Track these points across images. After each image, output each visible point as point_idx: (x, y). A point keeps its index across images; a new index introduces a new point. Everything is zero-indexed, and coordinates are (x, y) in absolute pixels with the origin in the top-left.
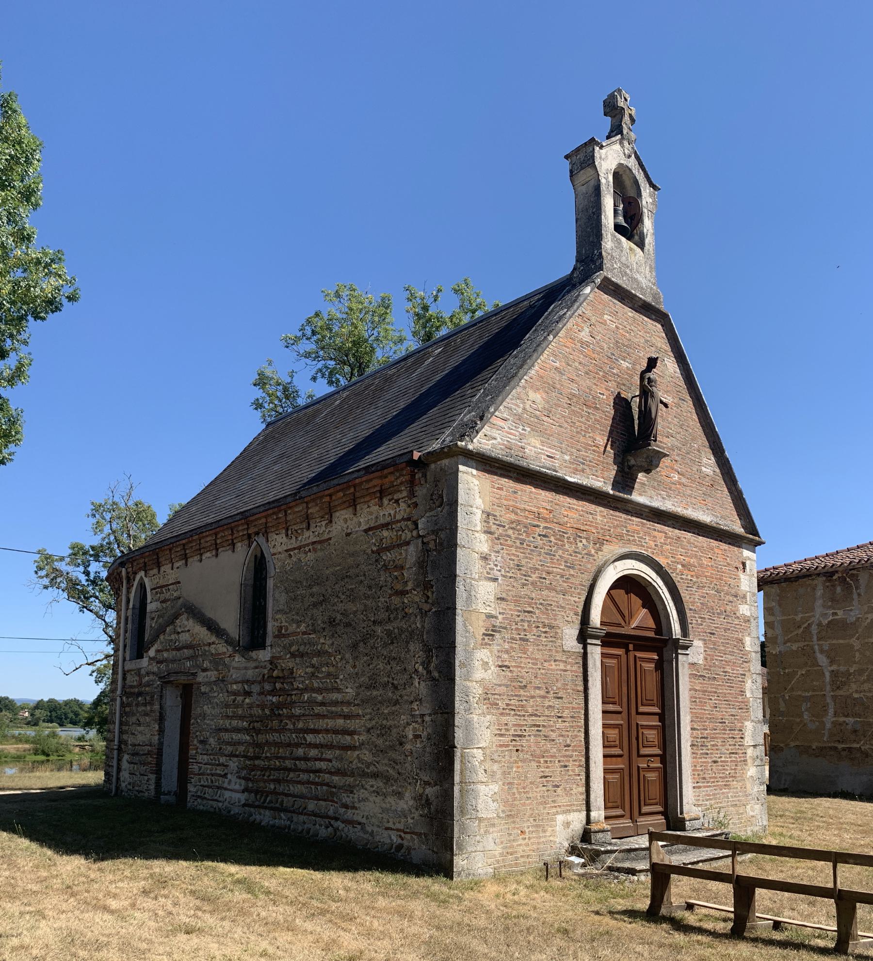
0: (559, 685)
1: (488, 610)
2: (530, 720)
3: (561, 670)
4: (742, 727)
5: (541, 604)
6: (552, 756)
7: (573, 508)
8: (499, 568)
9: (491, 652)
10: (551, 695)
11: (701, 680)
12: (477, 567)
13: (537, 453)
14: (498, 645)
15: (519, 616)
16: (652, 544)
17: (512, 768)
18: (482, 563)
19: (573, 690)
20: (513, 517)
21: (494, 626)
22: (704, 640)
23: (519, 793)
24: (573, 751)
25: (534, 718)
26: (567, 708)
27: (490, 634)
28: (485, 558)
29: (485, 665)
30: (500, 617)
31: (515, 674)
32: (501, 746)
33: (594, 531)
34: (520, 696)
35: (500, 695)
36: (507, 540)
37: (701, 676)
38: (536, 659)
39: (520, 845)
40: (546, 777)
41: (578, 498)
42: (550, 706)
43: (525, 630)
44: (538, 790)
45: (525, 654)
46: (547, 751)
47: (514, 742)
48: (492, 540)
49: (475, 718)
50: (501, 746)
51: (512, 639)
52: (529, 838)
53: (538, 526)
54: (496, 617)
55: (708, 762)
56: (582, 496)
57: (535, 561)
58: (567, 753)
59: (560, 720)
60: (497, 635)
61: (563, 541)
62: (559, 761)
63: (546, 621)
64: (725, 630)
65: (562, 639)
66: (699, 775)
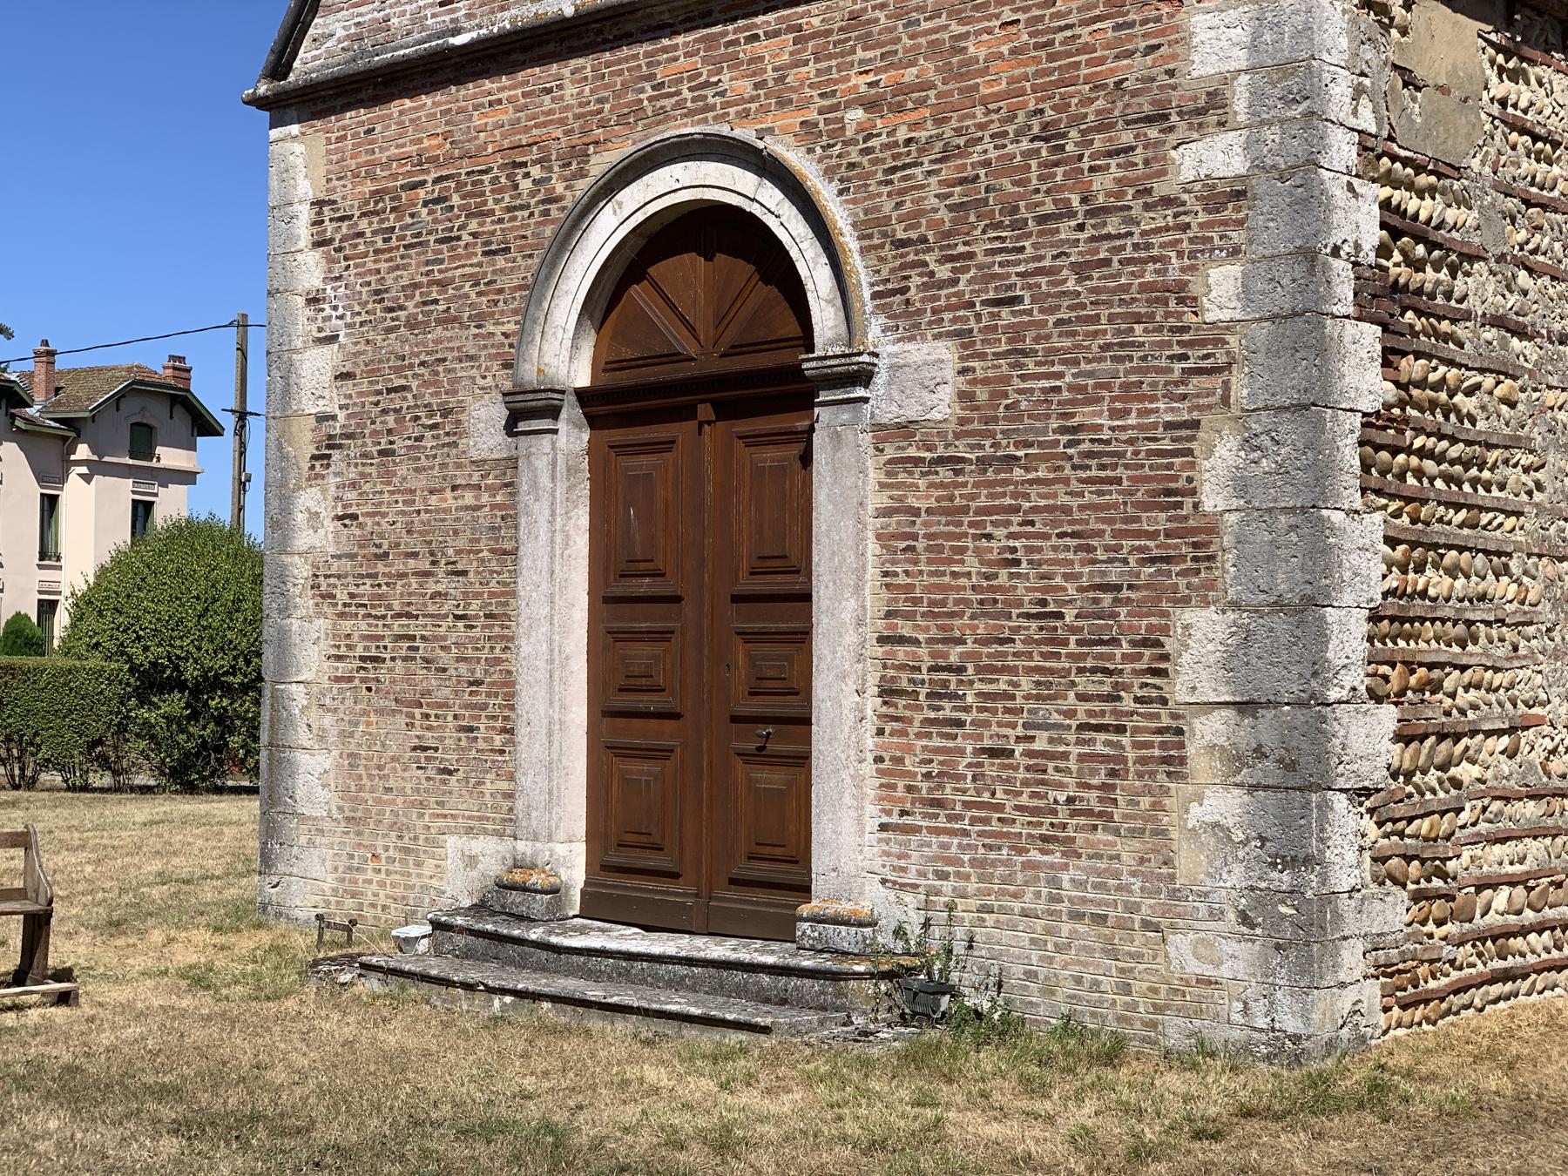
1: (322, 407)
2: (397, 626)
3: (467, 508)
4: (1165, 630)
5: (422, 364)
6: (440, 706)
7: (499, 102)
8: (341, 311)
9: (324, 491)
10: (441, 570)
11: (944, 474)
14: (336, 474)
15: (377, 404)
16: (746, 86)
17: (357, 724)
18: (309, 312)
19: (492, 551)
20: (368, 187)
21: (330, 437)
22: (958, 334)
23: (370, 776)
24: (488, 695)
25: (404, 621)
26: (478, 595)
28: (314, 301)
31: (369, 529)
32: (338, 679)
33: (559, 133)
34: (375, 576)
35: (339, 577)
36: (355, 246)
37: (941, 461)
38: (413, 492)
39: (370, 882)
40: (425, 749)
41: (511, 68)
42: (439, 594)
43: (390, 432)
44: (406, 774)
45: (389, 483)
46: (429, 692)
47: (362, 667)
48: (331, 261)
49: (295, 624)
50: (338, 679)
51: (365, 455)
52: (388, 873)
53: (423, 183)
54: (334, 418)
55: (961, 752)
56: (522, 57)
58: (474, 699)
59: (460, 624)
60: (336, 455)
61: (483, 194)
62: (455, 717)
63: (434, 401)
64: (1081, 271)
66: (909, 789)
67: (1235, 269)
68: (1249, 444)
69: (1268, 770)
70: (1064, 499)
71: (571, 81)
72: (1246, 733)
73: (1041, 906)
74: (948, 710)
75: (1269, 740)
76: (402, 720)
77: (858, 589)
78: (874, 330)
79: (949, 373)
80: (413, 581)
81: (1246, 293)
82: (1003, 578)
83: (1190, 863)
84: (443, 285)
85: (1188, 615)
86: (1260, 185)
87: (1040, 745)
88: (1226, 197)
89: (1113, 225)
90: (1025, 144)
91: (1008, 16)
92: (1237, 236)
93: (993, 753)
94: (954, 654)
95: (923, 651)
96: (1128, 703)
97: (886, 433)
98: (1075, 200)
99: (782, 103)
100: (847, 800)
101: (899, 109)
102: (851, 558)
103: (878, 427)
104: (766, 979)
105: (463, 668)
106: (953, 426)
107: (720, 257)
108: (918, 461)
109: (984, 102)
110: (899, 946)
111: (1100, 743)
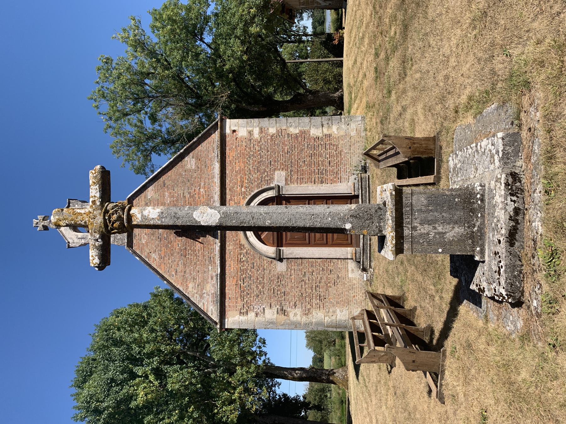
0: (300, 274)
1: (275, 313)
9: (291, 312)
12: (260, 318)
13: (212, 287)
20: (239, 299)
27: (283, 312)
28: (257, 315)
29: (295, 315)
30: (278, 307)
41: (225, 261)
48: (250, 310)
49: (314, 320)
57: (254, 287)
60: (284, 308)
64: (268, 151)
65: (282, 272)
67: (270, 129)
68: (291, 126)
69: (330, 122)
71: (229, 247)
72: (325, 126)
74: (324, 172)
75: (326, 122)
76: (330, 289)
78: (272, 185)
80: (306, 286)
81: (273, 127)
82: (306, 163)
83: (342, 133)
84: (257, 279)
85: (311, 134)
86: (260, 126)
88: (261, 131)
89: (263, 147)
92: (266, 129)
94: (317, 171)
96: (322, 143)
97: (286, 184)
104: (363, 192)
105: (321, 273)
110: (357, 179)
111: (328, 147)
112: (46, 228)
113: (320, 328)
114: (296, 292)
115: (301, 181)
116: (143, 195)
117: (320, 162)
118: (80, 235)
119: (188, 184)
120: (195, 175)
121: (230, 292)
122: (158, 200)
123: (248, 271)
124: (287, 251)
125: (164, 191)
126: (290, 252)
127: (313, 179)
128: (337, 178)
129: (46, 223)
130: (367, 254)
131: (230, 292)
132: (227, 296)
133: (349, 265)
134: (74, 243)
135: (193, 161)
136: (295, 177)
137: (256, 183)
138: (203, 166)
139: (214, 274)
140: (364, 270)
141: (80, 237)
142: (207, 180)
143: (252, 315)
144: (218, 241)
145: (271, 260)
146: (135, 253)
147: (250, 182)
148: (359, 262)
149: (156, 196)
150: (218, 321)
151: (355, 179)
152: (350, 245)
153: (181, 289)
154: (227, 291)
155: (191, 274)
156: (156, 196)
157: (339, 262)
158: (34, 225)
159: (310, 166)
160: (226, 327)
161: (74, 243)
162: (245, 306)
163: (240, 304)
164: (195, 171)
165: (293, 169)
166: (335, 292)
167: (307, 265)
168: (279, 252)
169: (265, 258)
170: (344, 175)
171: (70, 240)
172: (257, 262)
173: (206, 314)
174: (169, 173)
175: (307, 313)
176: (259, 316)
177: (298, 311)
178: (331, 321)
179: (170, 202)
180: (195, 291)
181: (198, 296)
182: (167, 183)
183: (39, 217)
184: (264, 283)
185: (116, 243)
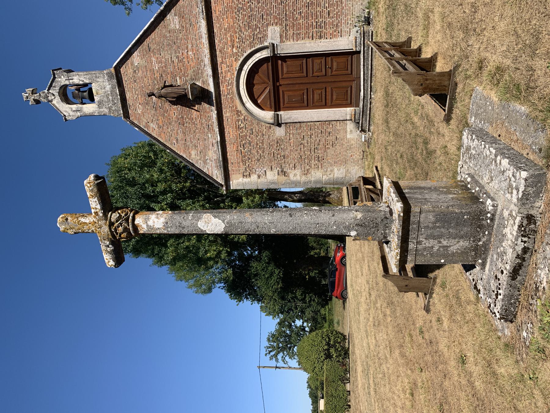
1: (276, 174)
11: (288, 28)
12: (262, 180)
13: (214, 153)
20: (241, 164)
27: (284, 173)
28: (259, 177)
29: (295, 175)
30: (278, 169)
49: (313, 179)
60: (284, 170)
70: (291, 4)
71: (226, 114)
73: (351, 3)
74: (323, 25)
76: (328, 150)
77: (305, 43)
78: (266, 44)
79: (273, 28)
82: (303, 15)
84: (257, 144)
87: (327, 5)
90: (240, 15)
91: (222, 20)
93: (329, 15)
94: (314, 24)
95: (314, 30)
97: (282, 41)
98: (248, 4)
99: (232, 66)
100: (337, 43)
101: (234, 41)
102: (300, 45)
103: (281, 42)
104: (366, 49)
105: (319, 136)
106: (281, 27)
107: (254, 82)
108: (286, 33)
109: (234, 24)
112: (37, 102)
113: (318, 186)
114: (295, 155)
115: (297, 37)
116: (129, 62)
117: (318, 13)
118: (74, 107)
119: (175, 47)
120: (181, 35)
121: (232, 157)
122: (146, 66)
123: (248, 137)
124: (286, 115)
125: (151, 57)
126: (288, 116)
127: (311, 34)
128: (338, 32)
129: (36, 96)
130: (366, 115)
131: (232, 157)
132: (229, 162)
133: (348, 127)
134: (70, 116)
135: (177, 19)
136: (291, 32)
137: (248, 42)
138: (188, 25)
139: (214, 141)
140: (363, 130)
141: (74, 109)
142: (194, 42)
143: (254, 177)
144: (214, 108)
145: (269, 125)
146: (133, 123)
147: (242, 41)
148: (358, 123)
149: (143, 63)
150: (223, 184)
151: (357, 32)
152: (350, 105)
153: (184, 156)
154: (229, 157)
155: (191, 142)
156: (143, 63)
157: (338, 124)
158: (25, 99)
159: (308, 18)
160: (232, 188)
161: (70, 116)
162: (247, 169)
163: (242, 168)
164: (180, 31)
165: (288, 23)
166: (333, 152)
167: (305, 129)
168: (277, 117)
169: (263, 124)
170: (345, 29)
171: (65, 114)
172: (256, 128)
173: (211, 178)
174: (153, 36)
175: (306, 173)
176: (261, 177)
177: (298, 172)
178: (329, 179)
179: (159, 68)
180: (199, 158)
181: (202, 162)
182: (153, 47)
183: (27, 90)
184: (264, 148)
185: (112, 115)
